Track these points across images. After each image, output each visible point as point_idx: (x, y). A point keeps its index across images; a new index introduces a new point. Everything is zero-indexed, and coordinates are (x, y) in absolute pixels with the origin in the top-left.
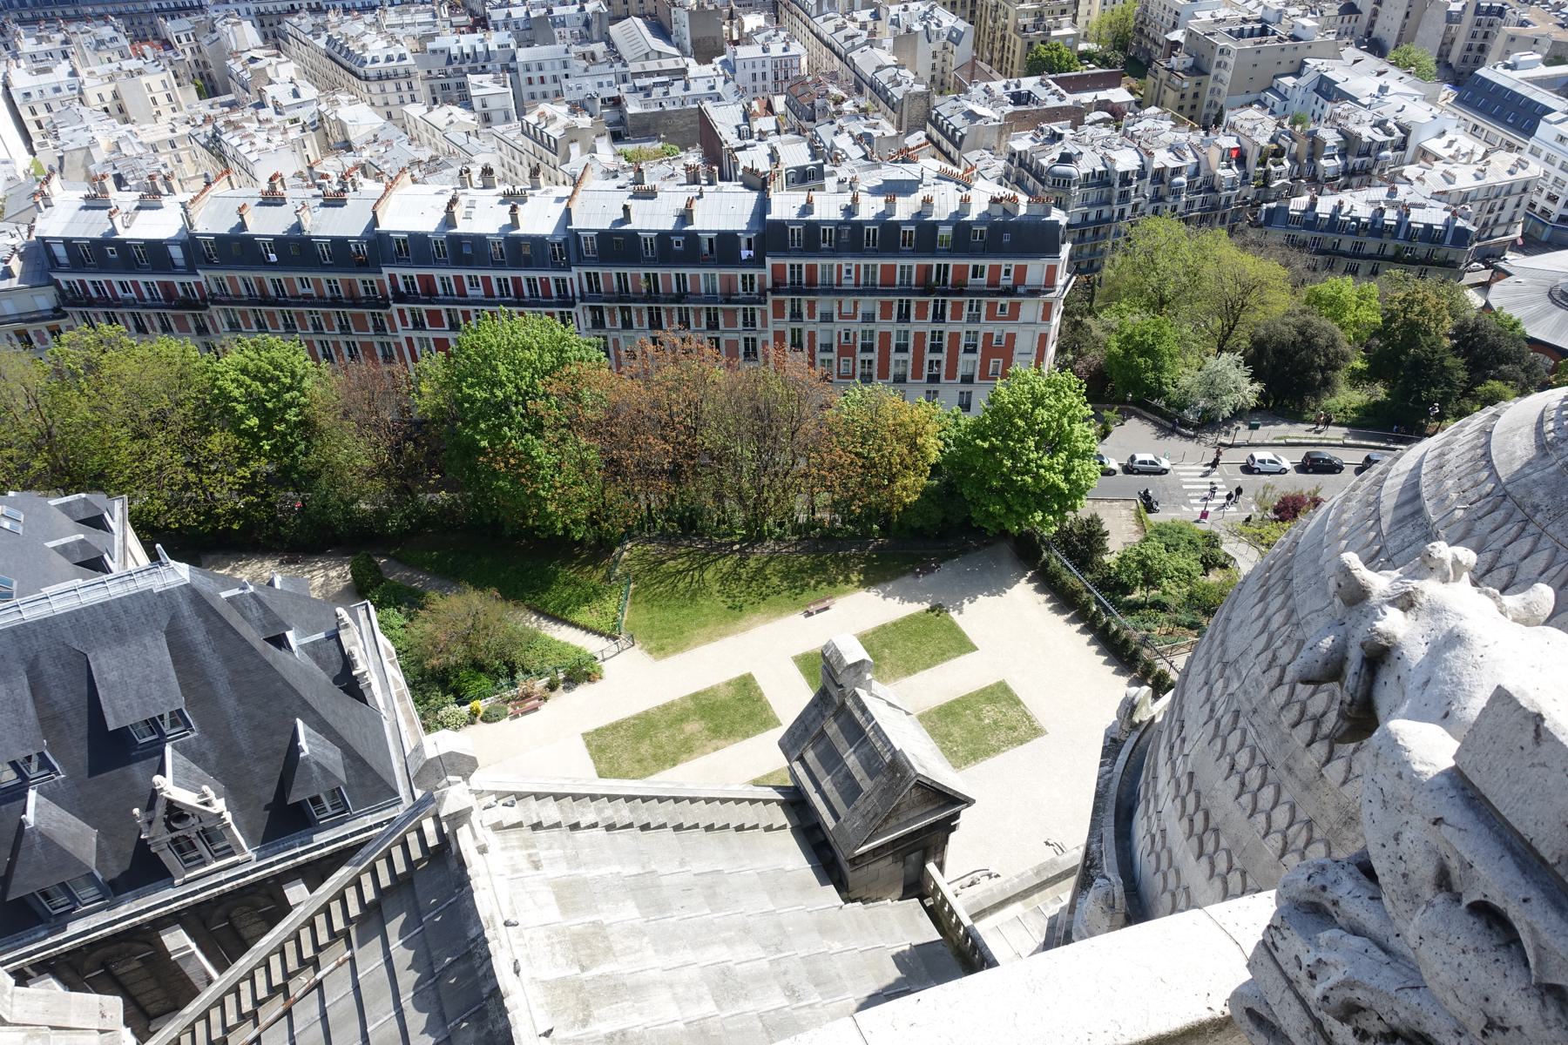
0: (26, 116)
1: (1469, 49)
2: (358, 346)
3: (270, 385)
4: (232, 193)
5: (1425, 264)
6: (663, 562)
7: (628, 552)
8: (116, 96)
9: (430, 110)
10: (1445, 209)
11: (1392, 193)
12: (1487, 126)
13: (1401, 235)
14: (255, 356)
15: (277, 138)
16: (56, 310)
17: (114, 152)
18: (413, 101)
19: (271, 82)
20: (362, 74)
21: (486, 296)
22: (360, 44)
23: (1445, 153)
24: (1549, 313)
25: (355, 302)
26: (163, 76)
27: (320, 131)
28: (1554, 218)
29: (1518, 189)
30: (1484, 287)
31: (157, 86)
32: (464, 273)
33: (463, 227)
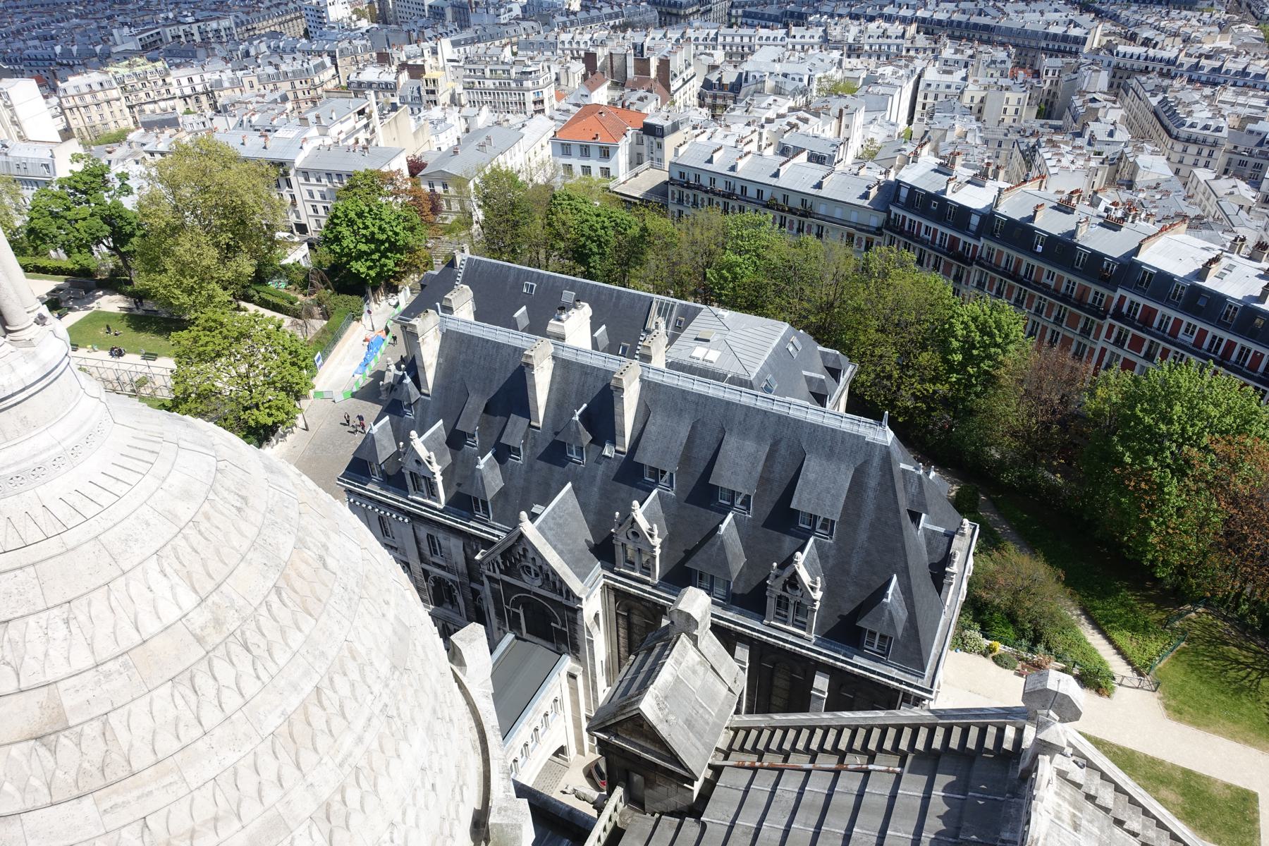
0: (920, 99)
2: (1060, 337)
3: (985, 338)
4: (1037, 193)
6: (1227, 644)
7: (1196, 615)
8: (982, 101)
9: (1217, 178)
14: (989, 313)
15: (1080, 162)
16: (879, 229)
17: (960, 138)
18: (1206, 166)
19: (1097, 120)
20: (1175, 133)
21: (1194, 345)
22: (1188, 109)
25: (1080, 304)
26: (1022, 95)
27: (1115, 167)
31: (1013, 101)
32: (1186, 319)
33: (1210, 283)
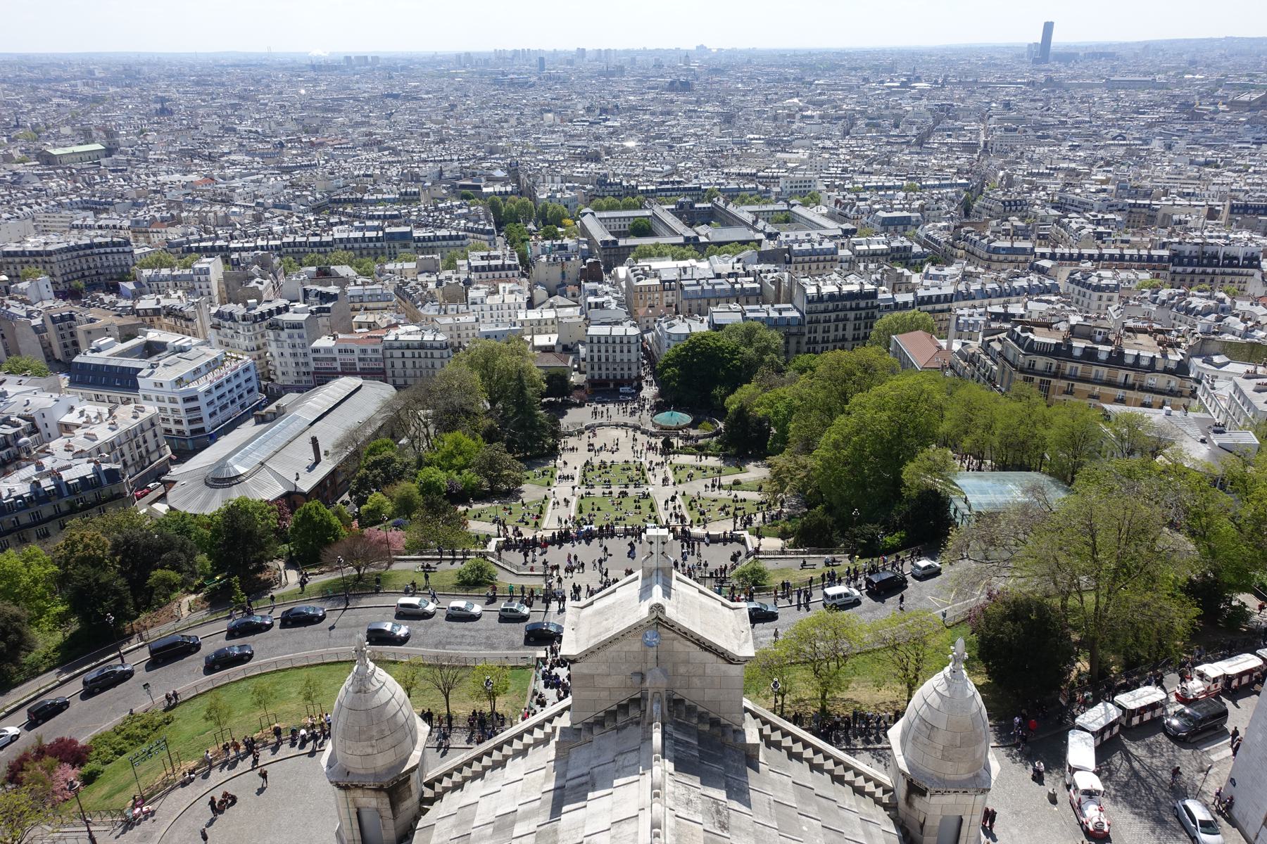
1: (66, 346)
5: (99, 504)
10: (89, 462)
11: (40, 467)
12: (105, 394)
13: (65, 492)
23: (80, 421)
24: (213, 495)
28: (187, 433)
29: (148, 426)
30: (162, 498)
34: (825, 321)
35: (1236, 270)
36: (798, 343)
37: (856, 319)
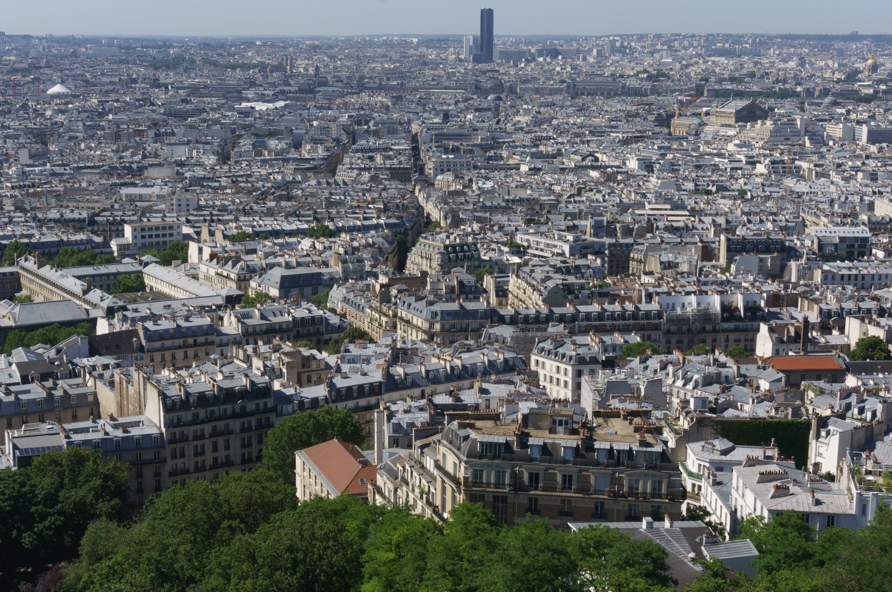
34: (196, 438)
35: (740, 324)
36: (157, 474)
37: (243, 430)
